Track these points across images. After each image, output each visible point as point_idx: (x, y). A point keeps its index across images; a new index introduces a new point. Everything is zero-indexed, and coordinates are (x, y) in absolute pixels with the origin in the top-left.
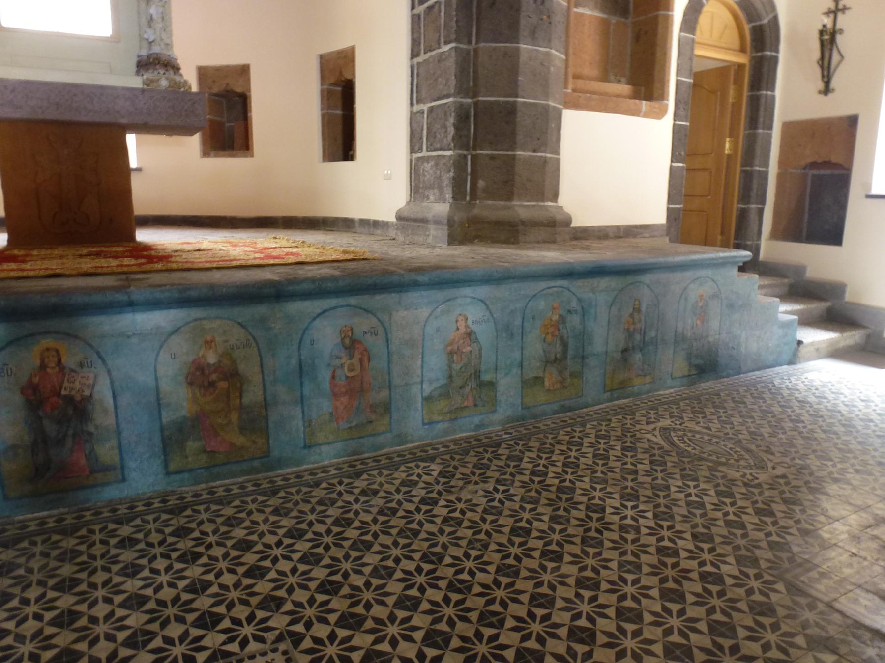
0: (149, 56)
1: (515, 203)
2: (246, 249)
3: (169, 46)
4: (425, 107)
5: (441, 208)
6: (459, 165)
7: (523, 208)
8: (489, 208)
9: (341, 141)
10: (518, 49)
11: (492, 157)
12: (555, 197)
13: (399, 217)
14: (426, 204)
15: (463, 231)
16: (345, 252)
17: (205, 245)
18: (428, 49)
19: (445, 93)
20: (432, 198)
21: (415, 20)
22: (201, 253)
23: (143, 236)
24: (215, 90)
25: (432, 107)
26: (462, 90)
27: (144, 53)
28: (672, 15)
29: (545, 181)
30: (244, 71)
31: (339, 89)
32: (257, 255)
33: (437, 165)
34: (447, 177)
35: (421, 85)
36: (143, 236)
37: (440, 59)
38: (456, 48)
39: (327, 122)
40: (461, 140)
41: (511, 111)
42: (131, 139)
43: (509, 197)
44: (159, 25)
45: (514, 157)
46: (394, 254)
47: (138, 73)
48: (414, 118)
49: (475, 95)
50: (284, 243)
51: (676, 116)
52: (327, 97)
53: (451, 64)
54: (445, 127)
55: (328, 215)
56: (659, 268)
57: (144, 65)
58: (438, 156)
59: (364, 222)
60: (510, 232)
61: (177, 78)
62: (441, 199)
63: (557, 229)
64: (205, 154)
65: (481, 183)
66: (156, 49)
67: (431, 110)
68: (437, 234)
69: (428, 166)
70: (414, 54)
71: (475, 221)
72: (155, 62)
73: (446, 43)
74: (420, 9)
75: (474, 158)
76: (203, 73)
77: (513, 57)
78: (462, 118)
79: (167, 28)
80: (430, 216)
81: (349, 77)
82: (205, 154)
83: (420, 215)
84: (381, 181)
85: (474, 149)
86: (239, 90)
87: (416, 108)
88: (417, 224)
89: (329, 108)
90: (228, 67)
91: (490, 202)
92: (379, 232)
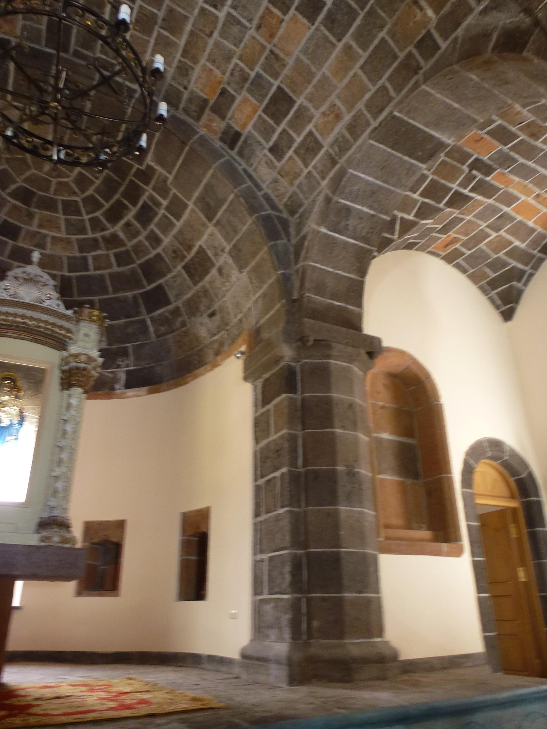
0: (49, 518)
1: (347, 641)
2: (103, 695)
3: (65, 510)
4: (266, 556)
5: (280, 647)
6: (295, 606)
9: (194, 582)
10: (337, 511)
11: (324, 599)
13: (245, 656)
14: (267, 643)
16: (194, 699)
17: (65, 690)
18: (268, 511)
19: (281, 546)
20: (273, 637)
21: (258, 489)
22: (61, 701)
24: (96, 540)
25: (273, 556)
26: (296, 543)
27: (45, 515)
28: (451, 478)
29: (370, 619)
30: (120, 525)
31: (195, 539)
32: (112, 704)
33: (276, 607)
34: (286, 618)
35: (262, 539)
37: (278, 519)
38: (289, 511)
39: (184, 566)
40: (296, 585)
41: (336, 560)
42: (19, 585)
43: (341, 635)
44: (60, 495)
45: (341, 599)
46: (238, 699)
47: (37, 532)
48: (257, 565)
49: (306, 547)
50: (136, 686)
51: (473, 554)
52: (186, 546)
53: (286, 523)
54: (282, 574)
55: (180, 651)
56: (488, 706)
57: (44, 524)
58: (278, 599)
59: (212, 659)
60: (343, 671)
61: (68, 535)
62: (280, 639)
63: (387, 666)
64: (79, 593)
65: (316, 624)
66: (56, 513)
67: (271, 559)
68: (277, 674)
69: (268, 608)
70: (257, 514)
71: (311, 660)
73: (282, 507)
74: (261, 481)
75: (309, 600)
77: (334, 516)
78: (297, 565)
79: (66, 498)
80: (270, 654)
81: (204, 530)
82: (79, 593)
83: (261, 655)
84: (228, 620)
85: (309, 592)
86: (115, 540)
87: (260, 557)
88: (260, 663)
89: (188, 554)
91: (326, 641)
92: (224, 669)
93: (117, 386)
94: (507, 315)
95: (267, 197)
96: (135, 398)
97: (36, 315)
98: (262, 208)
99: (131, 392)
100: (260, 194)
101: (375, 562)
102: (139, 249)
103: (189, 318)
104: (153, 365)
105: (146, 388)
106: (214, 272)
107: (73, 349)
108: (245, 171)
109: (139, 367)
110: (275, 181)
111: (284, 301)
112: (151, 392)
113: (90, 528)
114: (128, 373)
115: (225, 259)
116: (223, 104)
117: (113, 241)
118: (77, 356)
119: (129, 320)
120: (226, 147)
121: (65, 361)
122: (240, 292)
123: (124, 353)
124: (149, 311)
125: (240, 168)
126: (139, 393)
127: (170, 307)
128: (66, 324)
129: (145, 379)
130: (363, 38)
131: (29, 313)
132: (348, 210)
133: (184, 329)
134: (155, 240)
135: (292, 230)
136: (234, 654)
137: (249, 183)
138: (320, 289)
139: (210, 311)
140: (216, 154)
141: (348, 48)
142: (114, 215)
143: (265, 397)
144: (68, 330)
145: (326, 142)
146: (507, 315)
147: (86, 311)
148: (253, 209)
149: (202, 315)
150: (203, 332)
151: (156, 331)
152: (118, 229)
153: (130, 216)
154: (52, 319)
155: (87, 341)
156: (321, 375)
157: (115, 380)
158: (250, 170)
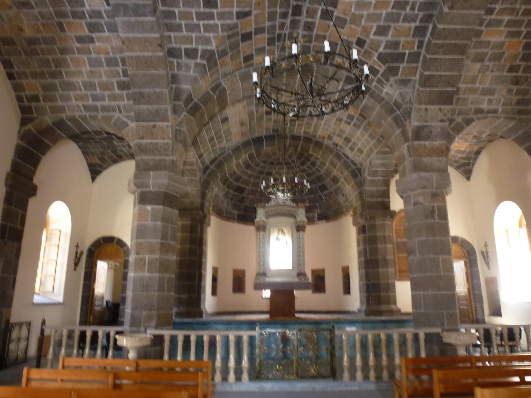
5: (364, 307)
7: (384, 307)
8: (375, 308)
9: (347, 290)
12: (395, 303)
15: (368, 313)
23: (297, 315)
30: (323, 270)
35: (360, 279)
36: (297, 315)
41: (378, 285)
60: (380, 313)
72: (301, 274)
76: (314, 272)
77: (378, 273)
78: (368, 286)
84: (355, 301)
94: (468, 179)
95: (353, 162)
97: (284, 208)
98: (350, 166)
99: (320, 222)
100: (349, 162)
101: (394, 285)
102: (314, 173)
106: (340, 183)
107: (298, 219)
108: (343, 154)
110: (353, 157)
113: (314, 272)
114: (318, 215)
115: (342, 179)
116: (330, 138)
117: (304, 171)
118: (300, 222)
120: (335, 146)
121: (296, 223)
122: (349, 191)
123: (316, 207)
125: (341, 154)
128: (294, 209)
129: (325, 217)
130: (366, 130)
131: (282, 208)
132: (377, 171)
134: (319, 171)
135: (362, 172)
136: (356, 309)
137: (344, 157)
138: (371, 196)
140: (331, 151)
141: (362, 132)
142: (303, 164)
143: (358, 234)
144: (295, 211)
145: (365, 151)
146: (468, 179)
147: (300, 204)
148: (347, 168)
150: (341, 201)
151: (326, 200)
152: (305, 167)
153: (308, 164)
154: (289, 208)
155: (302, 215)
156: (373, 227)
157: (314, 217)
158: (345, 153)
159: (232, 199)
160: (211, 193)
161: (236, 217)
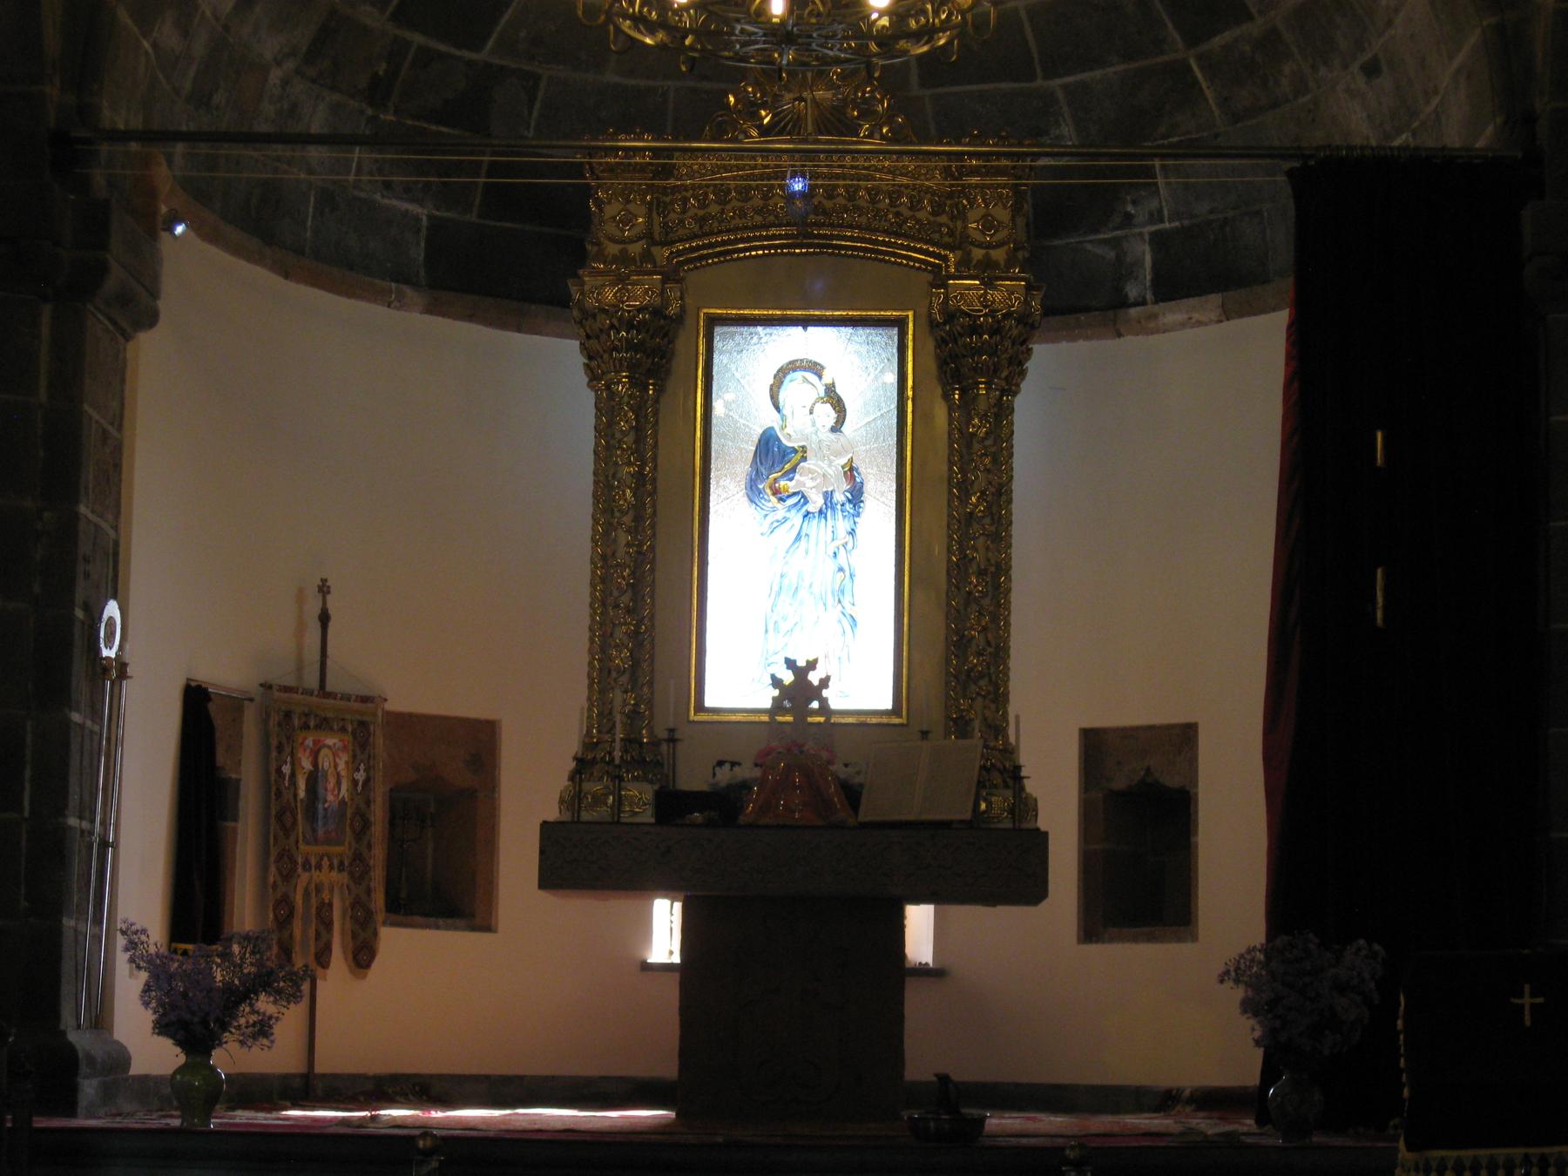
24: (1120, 784)
76: (1096, 746)
86: (1172, 781)
90: (1151, 728)
93: (1132, 291)
96: (1189, 333)
99: (1172, 314)
103: (1314, 67)
104: (1230, 214)
105: (1215, 299)
109: (1186, 222)
111: (1499, 120)
112: (1227, 314)
114: (1160, 242)
119: (1134, 65)
124: (1192, 40)
126: (1196, 316)
127: (1255, 28)
133: (1302, 100)
139: (1366, 57)
149: (1345, 67)
157: (1123, 270)
159: (377, 92)
160: (167, 33)
161: (418, 252)
